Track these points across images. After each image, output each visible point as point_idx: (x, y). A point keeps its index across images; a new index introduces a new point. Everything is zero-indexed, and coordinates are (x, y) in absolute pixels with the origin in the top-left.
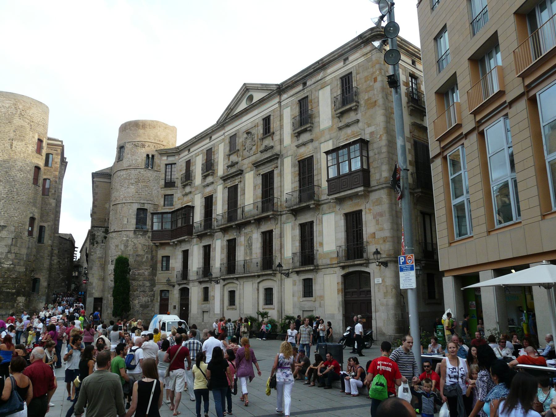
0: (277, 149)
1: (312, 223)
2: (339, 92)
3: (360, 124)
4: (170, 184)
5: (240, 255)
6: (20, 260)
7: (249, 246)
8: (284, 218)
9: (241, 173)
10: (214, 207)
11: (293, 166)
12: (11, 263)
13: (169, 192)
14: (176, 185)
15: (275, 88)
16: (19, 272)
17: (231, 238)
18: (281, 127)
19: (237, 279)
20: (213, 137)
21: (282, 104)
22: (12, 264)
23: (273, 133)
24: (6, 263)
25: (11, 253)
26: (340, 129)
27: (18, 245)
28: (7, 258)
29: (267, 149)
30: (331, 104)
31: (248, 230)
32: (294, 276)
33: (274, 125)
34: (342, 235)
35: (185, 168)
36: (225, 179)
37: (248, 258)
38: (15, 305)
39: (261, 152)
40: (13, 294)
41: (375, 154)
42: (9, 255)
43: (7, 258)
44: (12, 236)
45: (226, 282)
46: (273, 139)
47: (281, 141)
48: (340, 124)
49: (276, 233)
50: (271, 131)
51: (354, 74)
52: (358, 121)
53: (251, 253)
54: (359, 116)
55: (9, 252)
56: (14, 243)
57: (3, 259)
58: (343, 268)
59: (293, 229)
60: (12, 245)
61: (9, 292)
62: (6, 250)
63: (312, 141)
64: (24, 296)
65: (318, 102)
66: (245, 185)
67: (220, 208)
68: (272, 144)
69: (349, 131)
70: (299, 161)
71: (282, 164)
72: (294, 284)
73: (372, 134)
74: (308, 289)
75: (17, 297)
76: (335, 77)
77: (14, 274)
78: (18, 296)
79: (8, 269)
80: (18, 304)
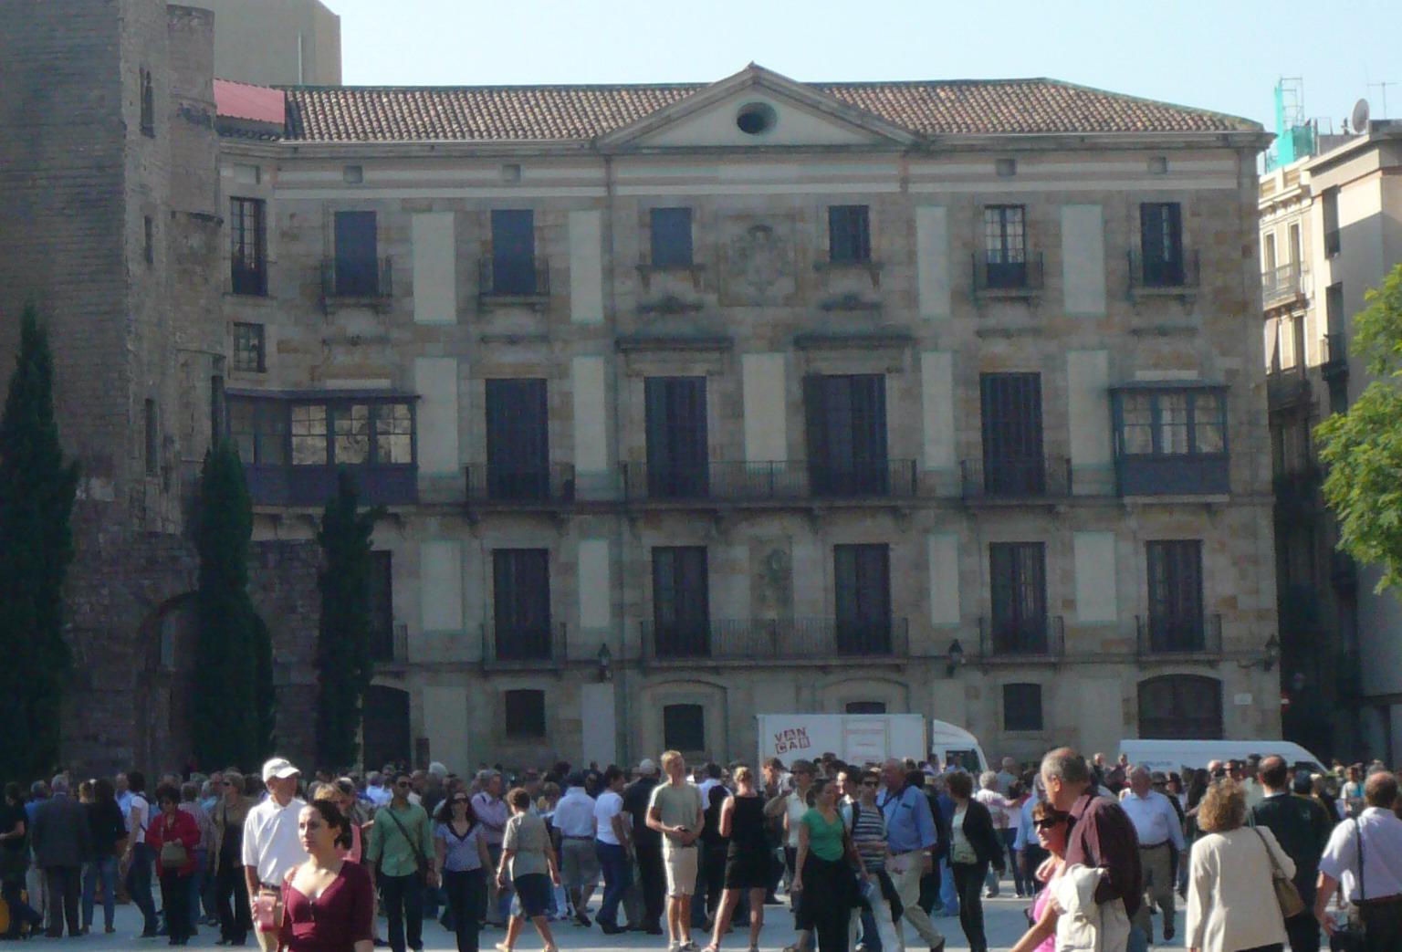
0: (898, 317)
1: (1039, 547)
2: (1136, 240)
3: (1199, 342)
4: (250, 280)
5: (732, 601)
7: (776, 577)
8: (927, 515)
9: (721, 344)
10: (553, 426)
11: (960, 380)
13: (249, 311)
14: (270, 287)
15: (906, 138)
17: (679, 543)
18: (911, 257)
19: (716, 670)
20: (529, 173)
21: (914, 188)
23: (880, 265)
26: (1136, 332)
29: (850, 303)
30: (1108, 256)
31: (770, 528)
32: (976, 678)
33: (881, 242)
34: (1138, 591)
35: (332, 237)
36: (623, 344)
37: (770, 615)
39: (827, 307)
41: (1241, 424)
45: (657, 678)
46: (876, 282)
47: (911, 298)
48: (1136, 322)
49: (899, 555)
50: (873, 255)
51: (1186, 213)
52: (1191, 332)
53: (785, 600)
54: (1196, 319)
58: (1142, 665)
59: (963, 551)
63: (1036, 332)
65: (1058, 236)
66: (740, 385)
67: (593, 431)
68: (870, 295)
69: (1165, 346)
70: (983, 376)
71: (917, 367)
72: (972, 693)
73: (1231, 373)
74: (1023, 710)
76: (1120, 192)
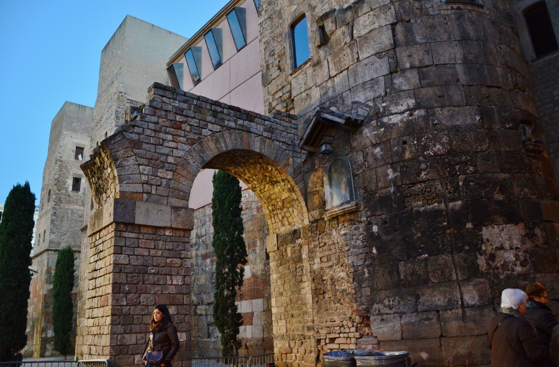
6: (446, 85)
12: (411, 102)
16: (456, 129)
22: (418, 106)
24: (394, 109)
25: (404, 71)
27: (418, 38)
28: (392, 93)
38: (482, 261)
40: (457, 219)
42: (398, 81)
43: (392, 93)
44: (389, 18)
55: (395, 69)
56: (400, 37)
57: (383, 98)
60: (395, 45)
61: (437, 213)
62: (382, 67)
64: (512, 218)
75: (478, 226)
77: (436, 139)
78: (479, 225)
79: (410, 128)
80: (492, 257)
